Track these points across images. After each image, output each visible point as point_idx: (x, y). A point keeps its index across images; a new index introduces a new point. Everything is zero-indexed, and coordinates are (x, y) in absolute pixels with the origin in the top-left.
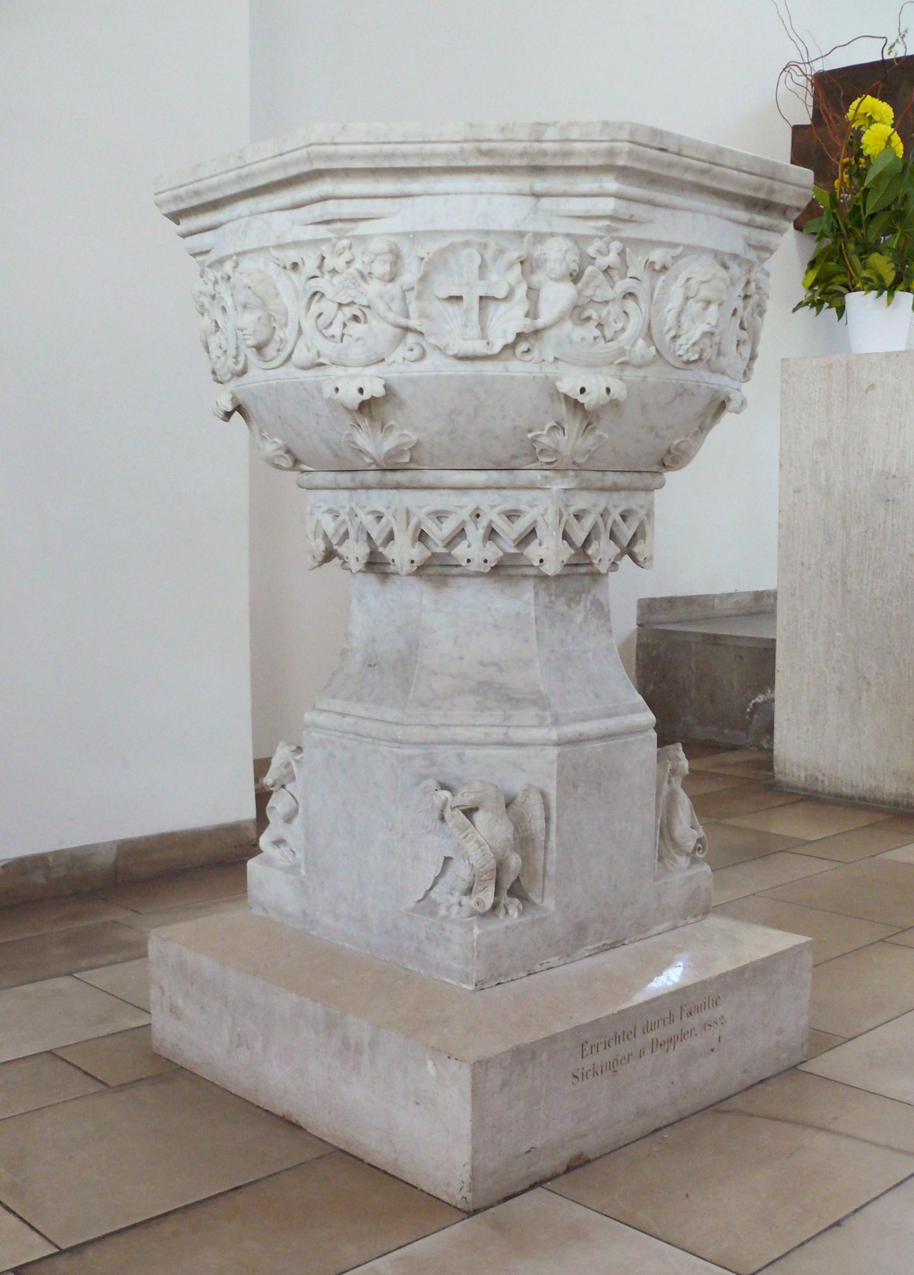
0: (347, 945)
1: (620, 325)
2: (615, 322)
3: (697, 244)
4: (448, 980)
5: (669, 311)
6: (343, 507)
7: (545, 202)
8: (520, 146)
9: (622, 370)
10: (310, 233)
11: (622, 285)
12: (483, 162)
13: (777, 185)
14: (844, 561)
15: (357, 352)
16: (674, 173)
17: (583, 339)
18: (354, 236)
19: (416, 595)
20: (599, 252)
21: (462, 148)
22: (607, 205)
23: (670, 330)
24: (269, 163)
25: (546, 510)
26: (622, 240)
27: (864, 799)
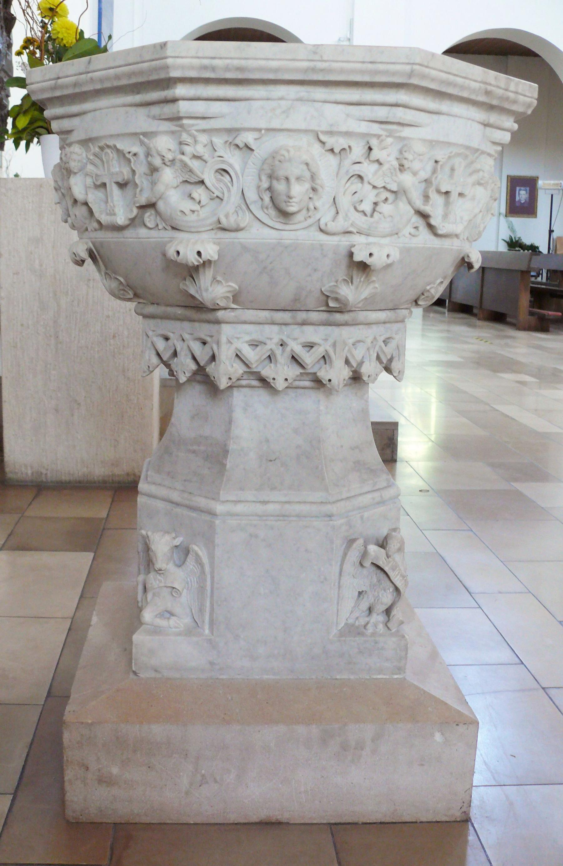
0: (265, 677)
4: (379, 677)
6: (271, 339)
7: (488, 129)
10: (363, 127)
12: (482, 98)
14: (55, 322)
15: (385, 226)
18: (400, 137)
19: (310, 401)
24: (359, 66)
27: (80, 482)
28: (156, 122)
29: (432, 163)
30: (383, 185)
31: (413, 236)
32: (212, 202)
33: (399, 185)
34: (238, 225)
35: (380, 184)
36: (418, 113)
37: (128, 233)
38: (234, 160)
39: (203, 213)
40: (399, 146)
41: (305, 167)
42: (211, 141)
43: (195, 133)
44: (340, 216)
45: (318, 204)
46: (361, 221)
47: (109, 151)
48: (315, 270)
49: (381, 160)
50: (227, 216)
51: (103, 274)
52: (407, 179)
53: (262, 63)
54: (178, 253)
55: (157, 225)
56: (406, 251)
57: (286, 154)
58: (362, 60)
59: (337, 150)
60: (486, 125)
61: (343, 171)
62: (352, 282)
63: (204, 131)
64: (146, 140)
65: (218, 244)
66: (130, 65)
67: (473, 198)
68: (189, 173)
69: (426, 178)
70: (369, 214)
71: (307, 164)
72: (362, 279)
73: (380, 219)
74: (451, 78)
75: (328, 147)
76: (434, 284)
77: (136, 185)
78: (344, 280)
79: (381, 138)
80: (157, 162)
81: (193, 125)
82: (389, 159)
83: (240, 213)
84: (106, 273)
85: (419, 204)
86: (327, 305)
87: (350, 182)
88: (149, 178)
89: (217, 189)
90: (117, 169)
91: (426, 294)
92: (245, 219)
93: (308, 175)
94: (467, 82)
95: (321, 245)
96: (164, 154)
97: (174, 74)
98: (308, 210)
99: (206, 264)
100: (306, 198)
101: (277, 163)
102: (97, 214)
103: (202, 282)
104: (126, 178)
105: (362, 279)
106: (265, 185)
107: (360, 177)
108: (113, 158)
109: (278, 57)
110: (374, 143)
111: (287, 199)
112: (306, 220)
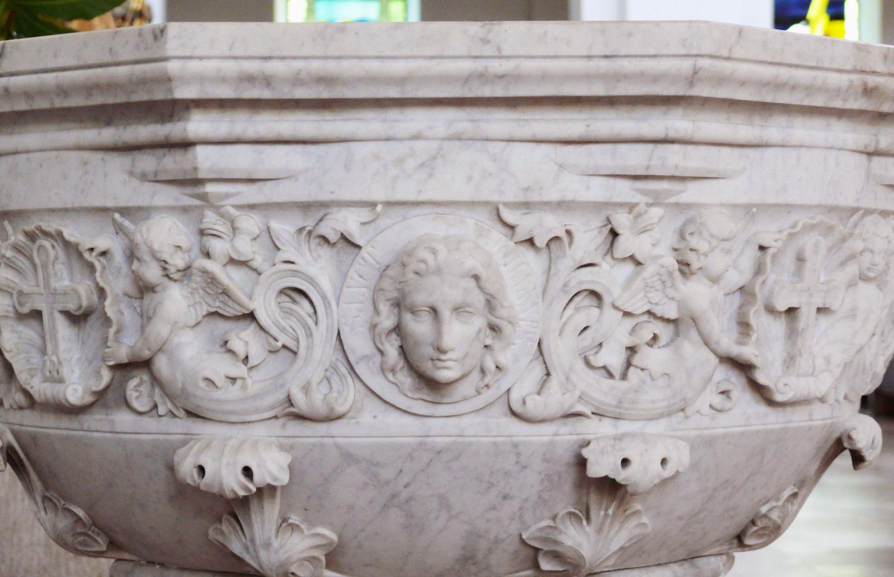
10: (597, 190)
15: (654, 396)
24: (579, 65)
28: (148, 187)
29: (752, 253)
30: (646, 309)
31: (720, 411)
32: (272, 357)
33: (681, 305)
34: (332, 410)
35: (638, 306)
36: (715, 149)
37: (95, 421)
38: (318, 268)
39: (256, 382)
40: (678, 223)
41: (472, 284)
42: (268, 228)
43: (233, 211)
44: (554, 383)
45: (504, 358)
46: (602, 390)
47: (47, 243)
48: (505, 497)
49: (639, 257)
50: (306, 389)
51: (39, 500)
52: (698, 294)
53: (373, 66)
54: (202, 470)
55: (156, 406)
56: (704, 444)
57: (430, 258)
58: (586, 54)
59: (540, 242)
60: (872, 153)
61: (556, 284)
62: (588, 519)
63: (252, 207)
64: (127, 223)
65: (289, 449)
66: (90, 67)
67: (852, 314)
68: (221, 298)
69: (740, 284)
70: (617, 374)
71: (476, 278)
72: (610, 512)
73: (643, 382)
74: (784, 73)
75: (521, 234)
76: (777, 500)
77: (107, 321)
78: (571, 514)
79: (636, 211)
80: (152, 273)
81: (227, 196)
82: (658, 251)
83: (335, 380)
84: (45, 498)
85: (729, 344)
86: (536, 566)
87: (572, 305)
88: (136, 303)
89: (283, 330)
90: (66, 283)
91: (760, 524)
92: (347, 395)
93: (478, 299)
94: (821, 75)
95: (515, 446)
96: (165, 257)
97: (183, 93)
98: (483, 371)
99: (266, 492)
100: (478, 349)
101: (411, 276)
102: (22, 376)
103: (257, 527)
104: (85, 303)
105: (610, 512)
106: (387, 321)
107: (594, 294)
108: (56, 258)
109: (405, 52)
110: (621, 220)
111: (435, 354)
112: (479, 393)
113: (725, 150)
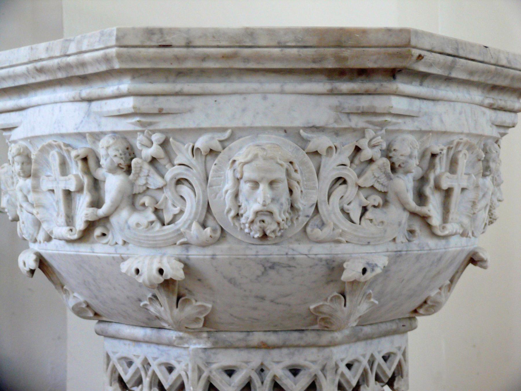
1: (176, 210)
2: (174, 206)
3: (248, 124)
5: (226, 192)
8: (56, 61)
9: (187, 250)
11: (171, 173)
13: (347, 53)
16: (189, 65)
17: (138, 225)
20: (143, 145)
21: (27, 68)
22: (128, 104)
23: (229, 210)
25: (187, 365)
26: (161, 131)
36: (8, 114)
60: (90, 100)
113: (12, 114)
